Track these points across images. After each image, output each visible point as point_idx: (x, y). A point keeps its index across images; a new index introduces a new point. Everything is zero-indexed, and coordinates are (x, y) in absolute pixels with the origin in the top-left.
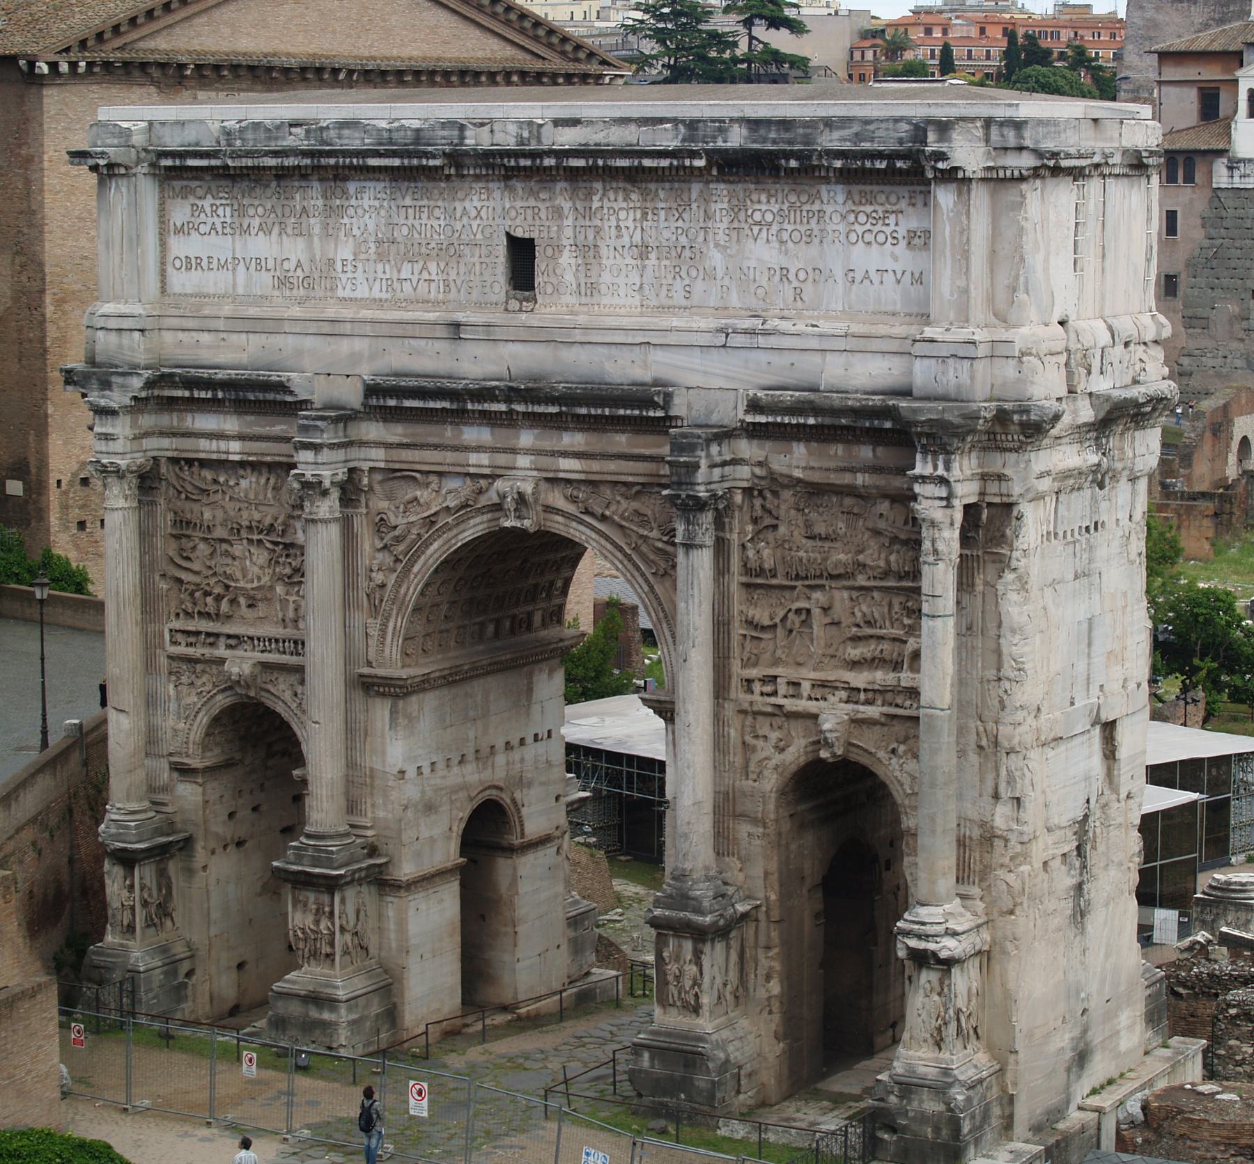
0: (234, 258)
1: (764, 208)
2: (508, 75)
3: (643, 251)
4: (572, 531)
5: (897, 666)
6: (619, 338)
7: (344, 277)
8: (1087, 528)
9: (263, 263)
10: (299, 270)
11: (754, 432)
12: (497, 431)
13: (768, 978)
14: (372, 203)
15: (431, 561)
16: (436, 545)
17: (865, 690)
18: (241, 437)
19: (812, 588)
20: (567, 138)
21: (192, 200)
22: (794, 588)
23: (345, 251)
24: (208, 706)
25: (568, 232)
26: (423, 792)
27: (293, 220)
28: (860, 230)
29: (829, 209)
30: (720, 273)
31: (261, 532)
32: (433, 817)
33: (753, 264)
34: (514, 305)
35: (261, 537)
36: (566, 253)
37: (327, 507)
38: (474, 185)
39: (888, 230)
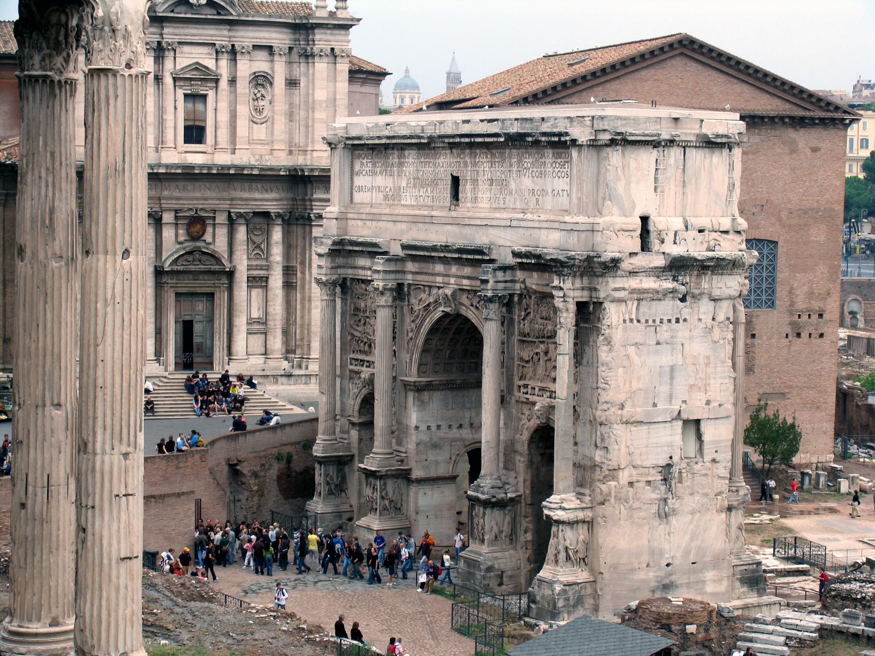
2: (782, 118)
3: (491, 181)
6: (479, 222)
8: (669, 321)
11: (522, 266)
13: (526, 532)
19: (542, 342)
20: (466, 129)
22: (535, 342)
23: (404, 184)
25: (469, 173)
26: (431, 439)
28: (557, 170)
29: (547, 161)
32: (438, 451)
33: (524, 187)
34: (453, 207)
37: (385, 300)
39: (565, 170)
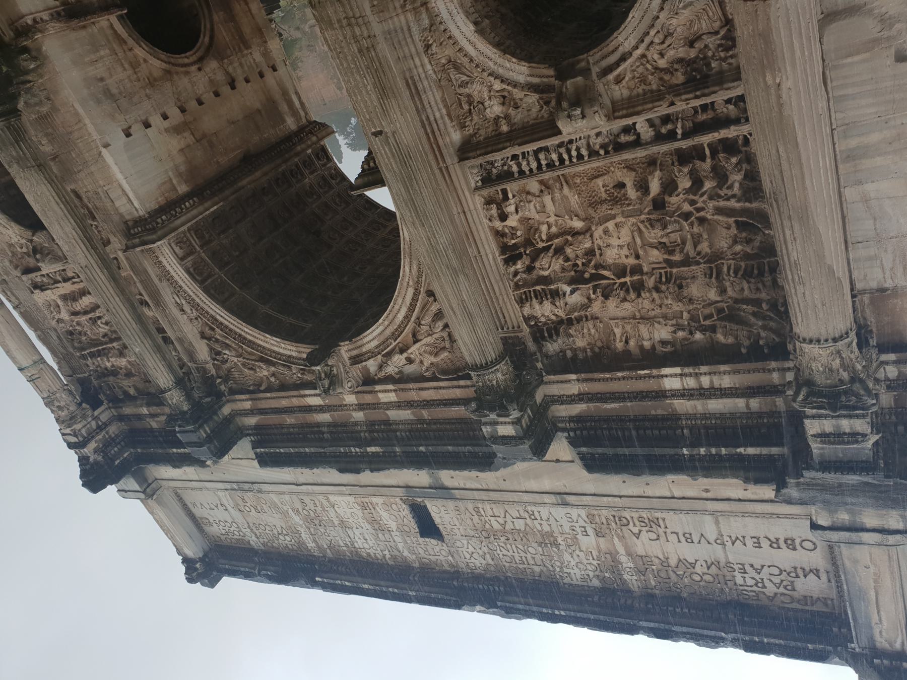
0: (723, 544)
1: (286, 542)
4: (294, 349)
5: (64, 298)
7: (582, 523)
9: (682, 539)
10: (636, 530)
12: (385, 418)
14: (571, 571)
15: (400, 300)
16: (400, 317)
17: (60, 282)
18: (661, 395)
21: (795, 594)
24: (647, 20)
25: (395, 538)
27: (654, 567)
30: (290, 511)
31: (623, 285)
35: (623, 280)
36: (393, 526)
38: (483, 572)
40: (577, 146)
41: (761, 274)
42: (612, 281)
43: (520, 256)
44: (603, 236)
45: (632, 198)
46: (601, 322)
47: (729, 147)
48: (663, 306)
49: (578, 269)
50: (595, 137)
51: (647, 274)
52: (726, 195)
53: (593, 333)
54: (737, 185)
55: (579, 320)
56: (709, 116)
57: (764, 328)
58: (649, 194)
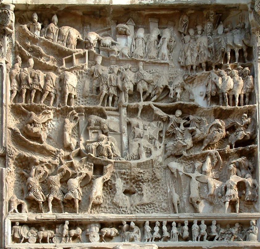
31: (148, 99)
35: (146, 103)
40: (152, 234)
41: (29, 92)
42: (157, 103)
43: (238, 143)
44: (152, 149)
45: (119, 179)
46: (180, 63)
47: (34, 205)
48: (116, 72)
49: (185, 121)
50: (135, 238)
51: (124, 106)
52: (43, 167)
53: (189, 51)
54: (33, 173)
55: (200, 67)
56: (41, 232)
57: (34, 40)
58: (104, 179)
